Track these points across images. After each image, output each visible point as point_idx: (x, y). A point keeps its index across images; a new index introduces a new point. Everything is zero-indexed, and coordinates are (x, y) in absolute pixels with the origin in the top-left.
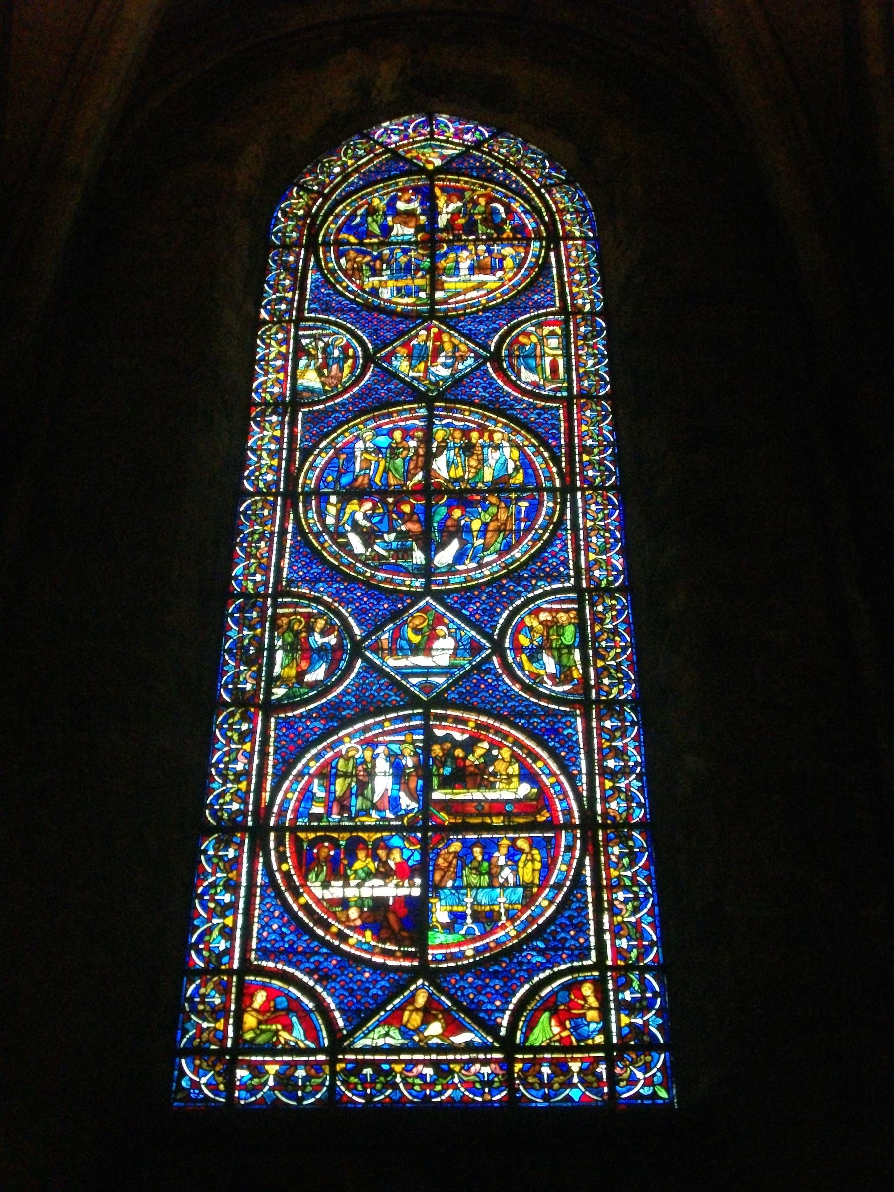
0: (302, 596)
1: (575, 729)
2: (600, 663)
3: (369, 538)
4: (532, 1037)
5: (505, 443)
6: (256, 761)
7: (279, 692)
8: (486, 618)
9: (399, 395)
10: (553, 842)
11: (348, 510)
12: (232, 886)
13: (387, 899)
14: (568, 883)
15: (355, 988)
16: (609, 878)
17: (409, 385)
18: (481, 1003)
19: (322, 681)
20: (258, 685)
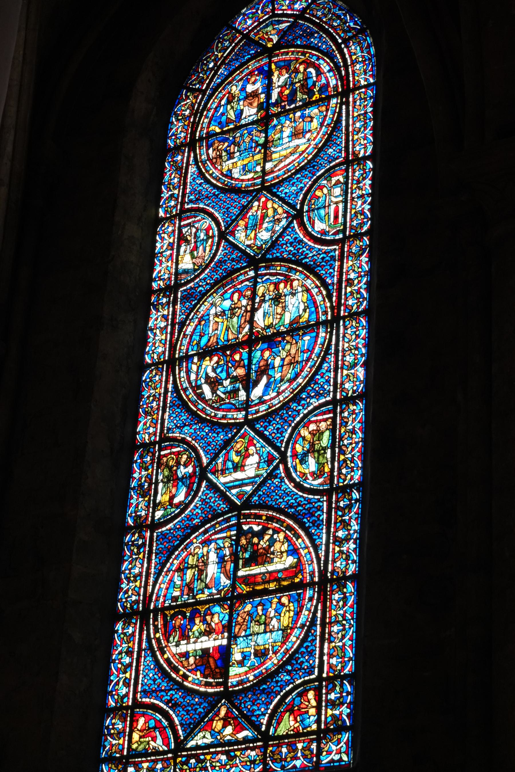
0: (175, 439)
1: (322, 511)
2: (342, 457)
3: (215, 386)
4: (279, 730)
5: (300, 289)
6: (145, 565)
7: (159, 514)
9: (238, 262)
10: (302, 596)
11: (203, 366)
12: (129, 653)
13: (210, 648)
14: (308, 624)
15: (190, 709)
16: (330, 617)
17: (244, 252)
18: (254, 711)
19: (183, 501)
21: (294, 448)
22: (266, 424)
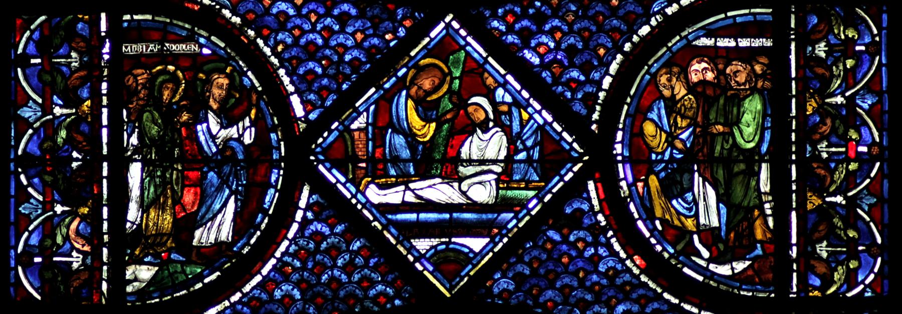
2: (813, 202)
8: (575, 74)
20: (96, 253)
21: (635, 137)
22: (525, 23)
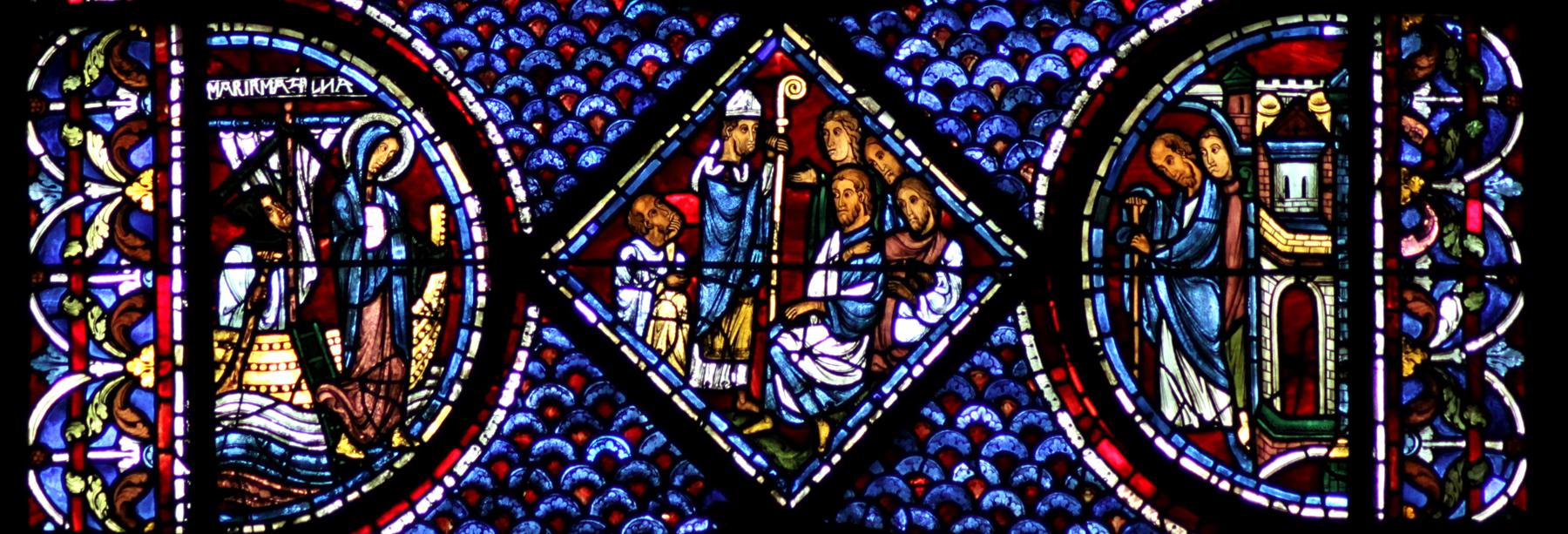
17: (688, 435)
